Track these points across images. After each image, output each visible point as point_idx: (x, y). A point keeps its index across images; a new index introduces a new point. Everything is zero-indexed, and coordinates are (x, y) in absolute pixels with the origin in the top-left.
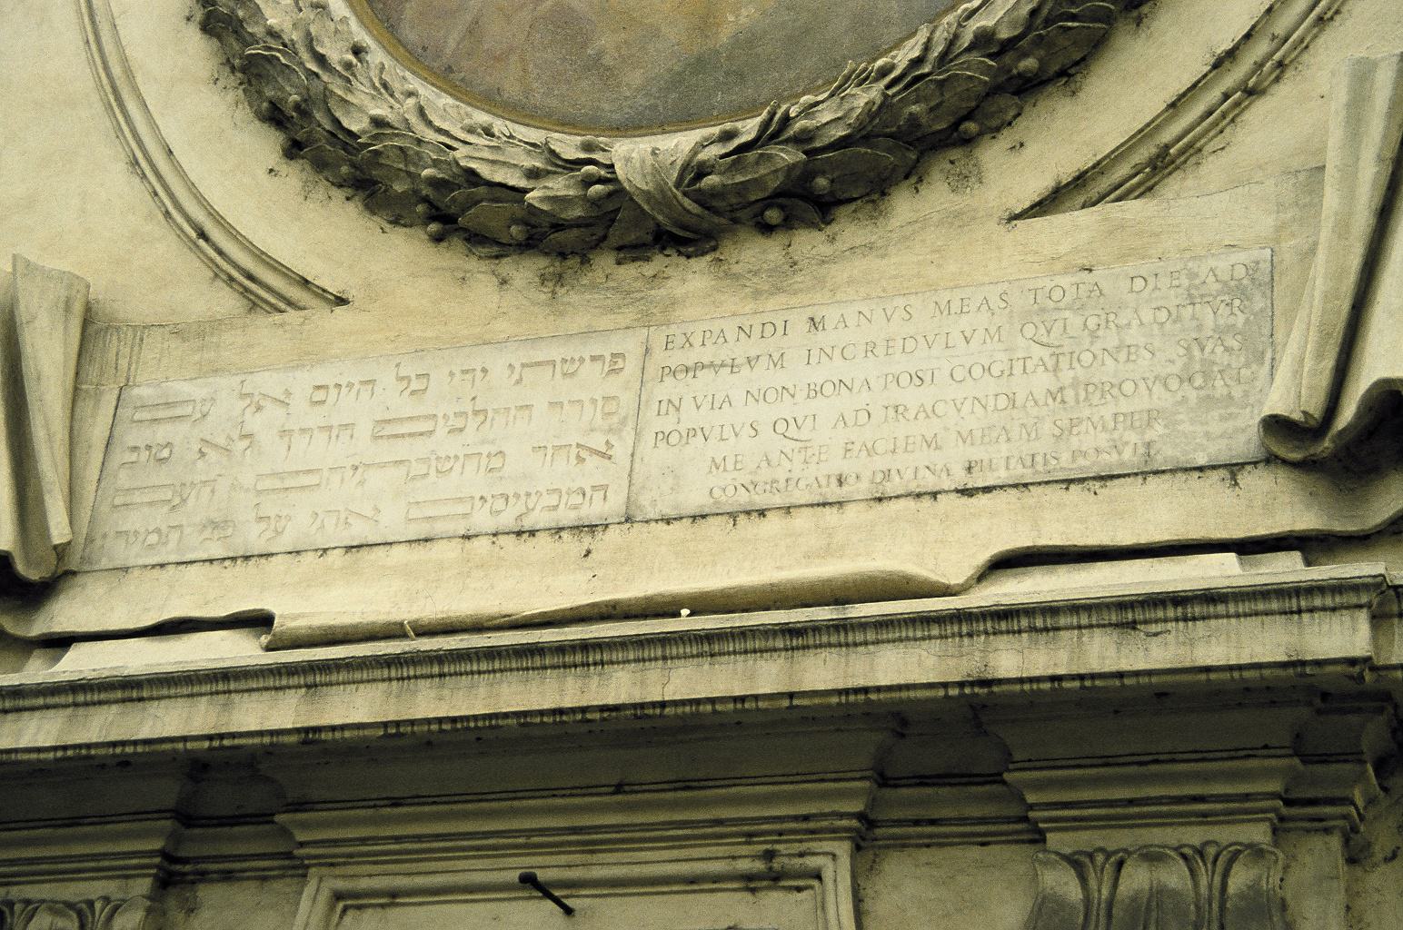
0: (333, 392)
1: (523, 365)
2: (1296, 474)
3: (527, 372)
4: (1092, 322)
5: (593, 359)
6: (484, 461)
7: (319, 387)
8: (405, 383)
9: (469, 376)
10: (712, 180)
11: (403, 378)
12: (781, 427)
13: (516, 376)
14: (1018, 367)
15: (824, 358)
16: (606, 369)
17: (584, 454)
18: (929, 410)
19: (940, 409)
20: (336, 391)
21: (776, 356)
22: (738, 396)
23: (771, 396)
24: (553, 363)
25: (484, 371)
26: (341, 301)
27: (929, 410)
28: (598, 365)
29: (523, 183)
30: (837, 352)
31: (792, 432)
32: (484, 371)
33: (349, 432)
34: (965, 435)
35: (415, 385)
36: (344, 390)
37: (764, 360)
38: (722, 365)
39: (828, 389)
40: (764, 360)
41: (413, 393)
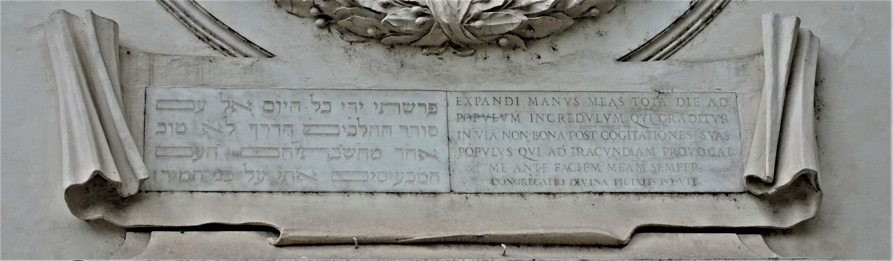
0: (277, 106)
1: (382, 104)
2: (757, 200)
3: (384, 108)
4: (663, 118)
5: (419, 104)
6: (370, 154)
7: (268, 102)
8: (317, 107)
9: (353, 106)
10: (478, 23)
11: (315, 103)
12: (523, 152)
13: (379, 109)
14: (632, 136)
15: (539, 120)
16: (428, 111)
17: (423, 155)
18: (593, 152)
19: (599, 151)
20: (284, 106)
21: (515, 116)
22: (499, 134)
23: (515, 135)
24: (398, 104)
25: (361, 104)
26: (271, 56)
27: (593, 152)
28: (423, 108)
29: (380, 9)
30: (545, 118)
31: (529, 155)
32: (361, 104)
33: (290, 129)
34: (612, 166)
35: (323, 107)
36: (283, 106)
37: (509, 117)
38: (488, 117)
39: (543, 135)
40: (509, 117)
41: (323, 111)
